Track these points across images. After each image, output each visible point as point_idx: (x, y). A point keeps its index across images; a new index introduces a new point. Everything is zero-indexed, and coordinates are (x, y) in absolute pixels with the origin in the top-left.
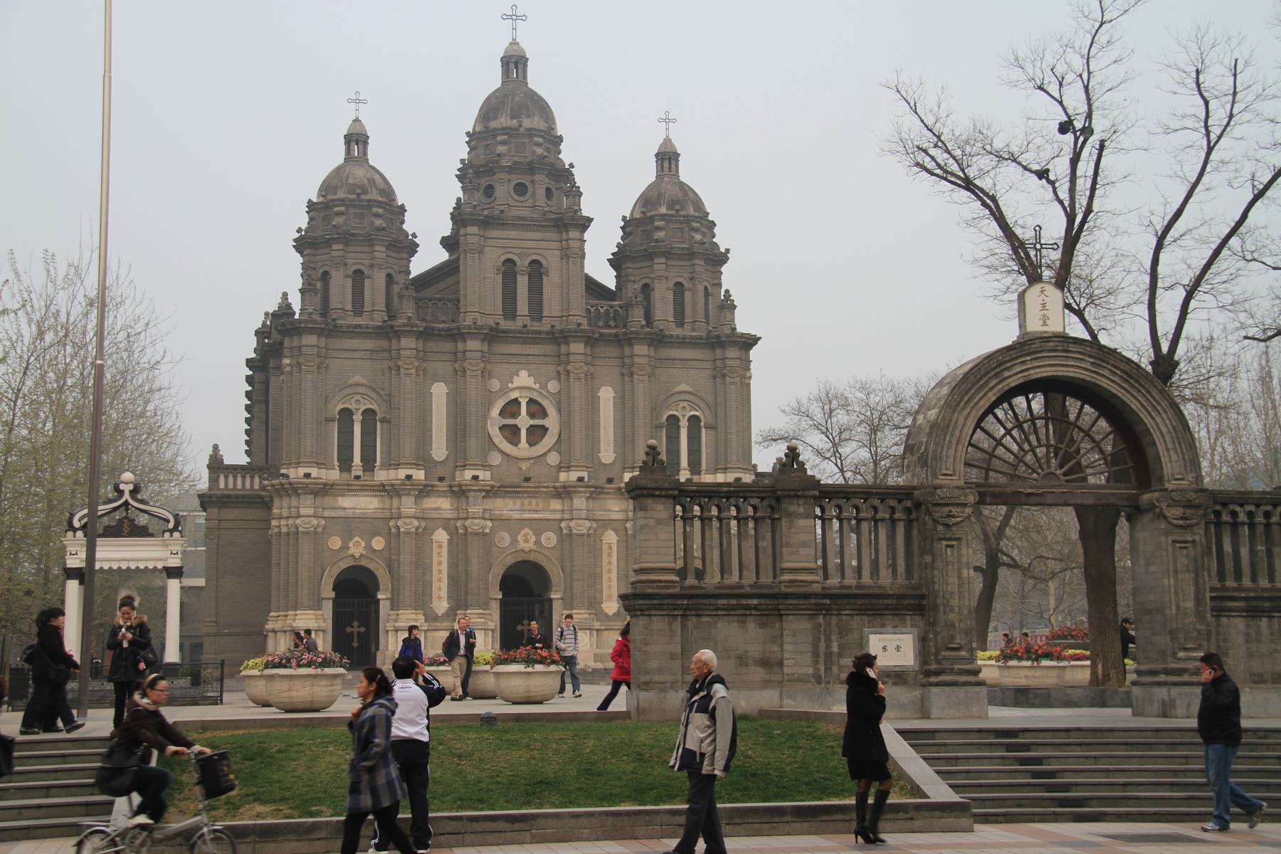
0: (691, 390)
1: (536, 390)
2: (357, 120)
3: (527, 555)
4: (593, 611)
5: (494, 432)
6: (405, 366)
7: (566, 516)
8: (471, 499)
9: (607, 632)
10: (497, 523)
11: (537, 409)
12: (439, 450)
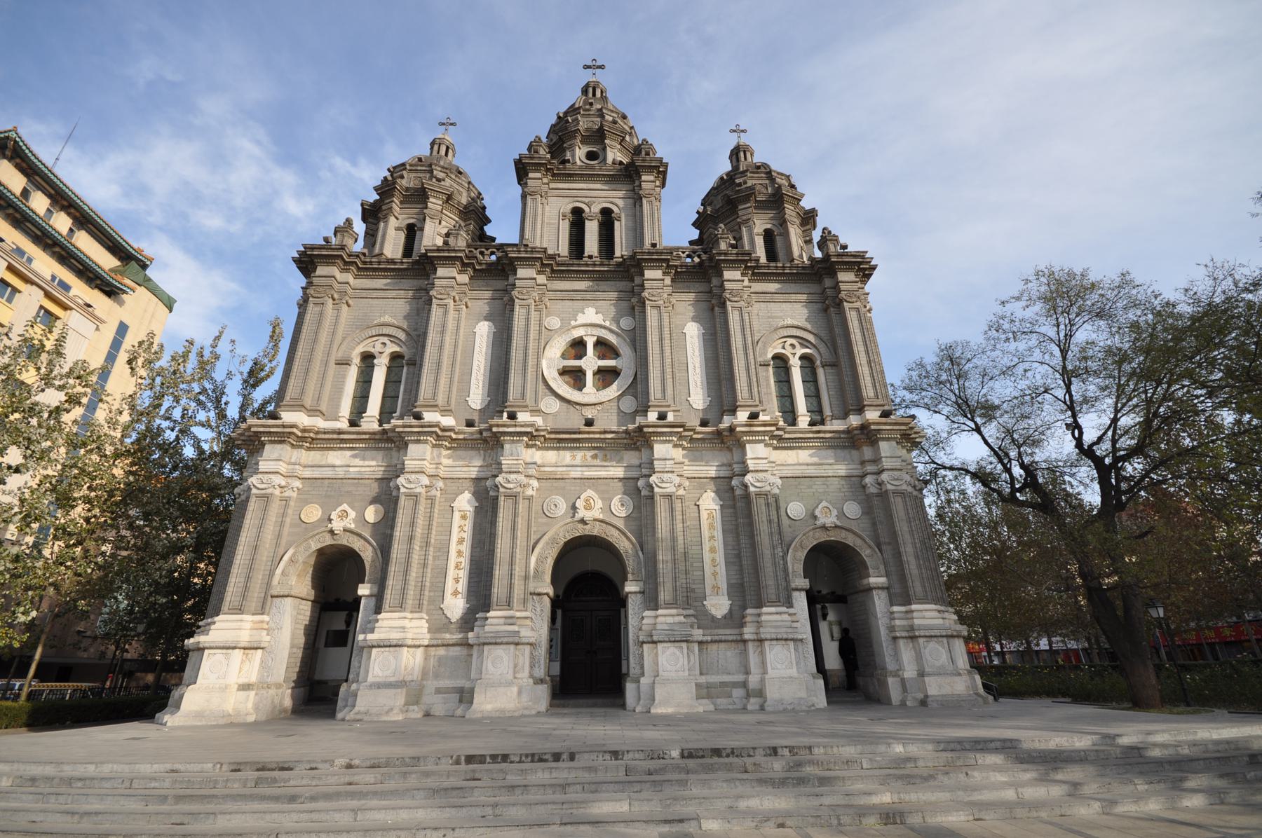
0: (796, 323)
1: (605, 328)
3: (587, 527)
4: (691, 612)
5: (552, 375)
6: (439, 297)
7: (645, 471)
8: (507, 446)
9: (715, 646)
10: (545, 483)
11: (604, 347)
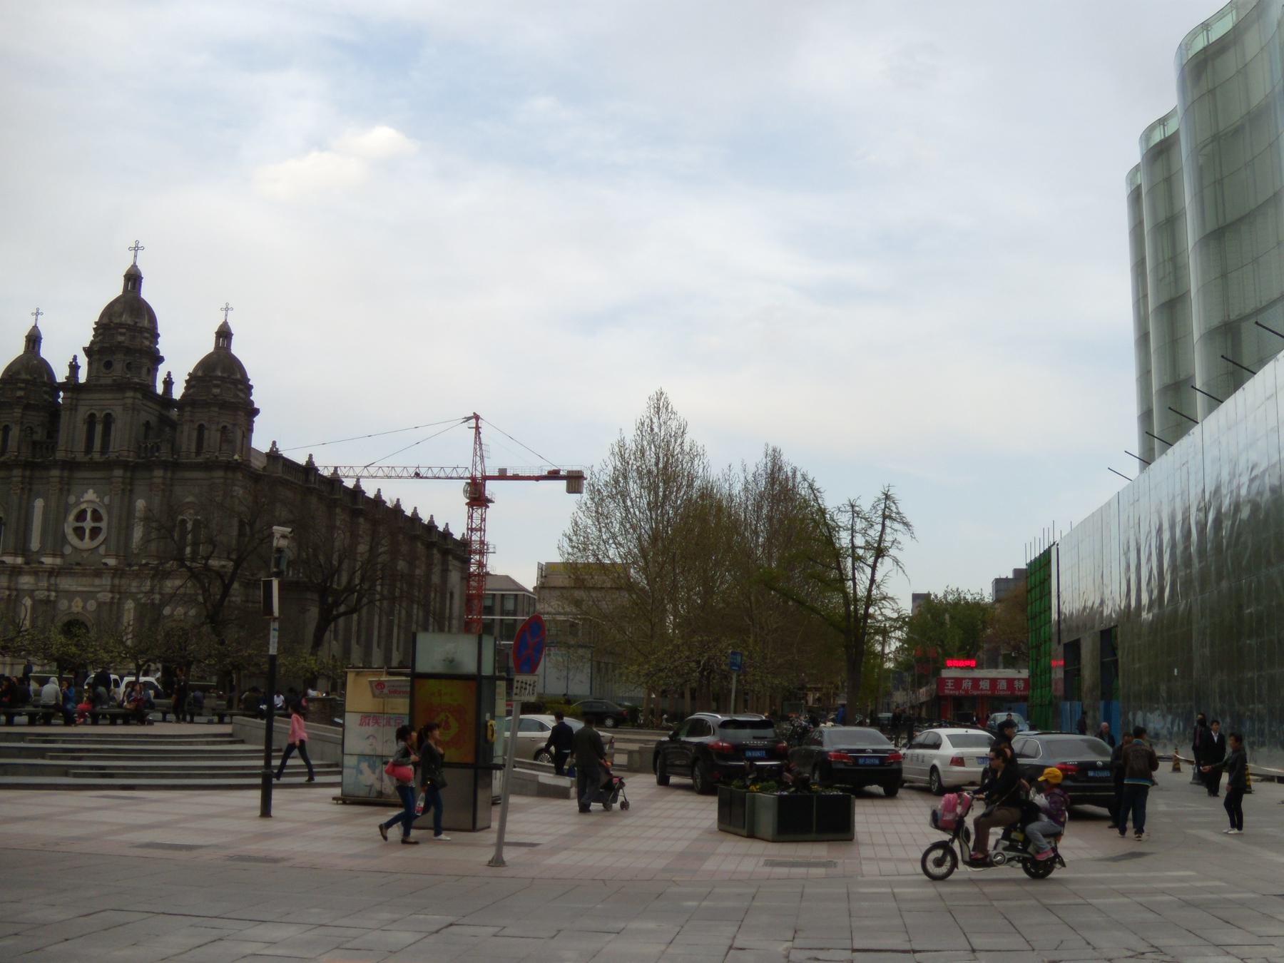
2: (35, 327)
5: (69, 531)
11: (97, 516)
12: (35, 545)
